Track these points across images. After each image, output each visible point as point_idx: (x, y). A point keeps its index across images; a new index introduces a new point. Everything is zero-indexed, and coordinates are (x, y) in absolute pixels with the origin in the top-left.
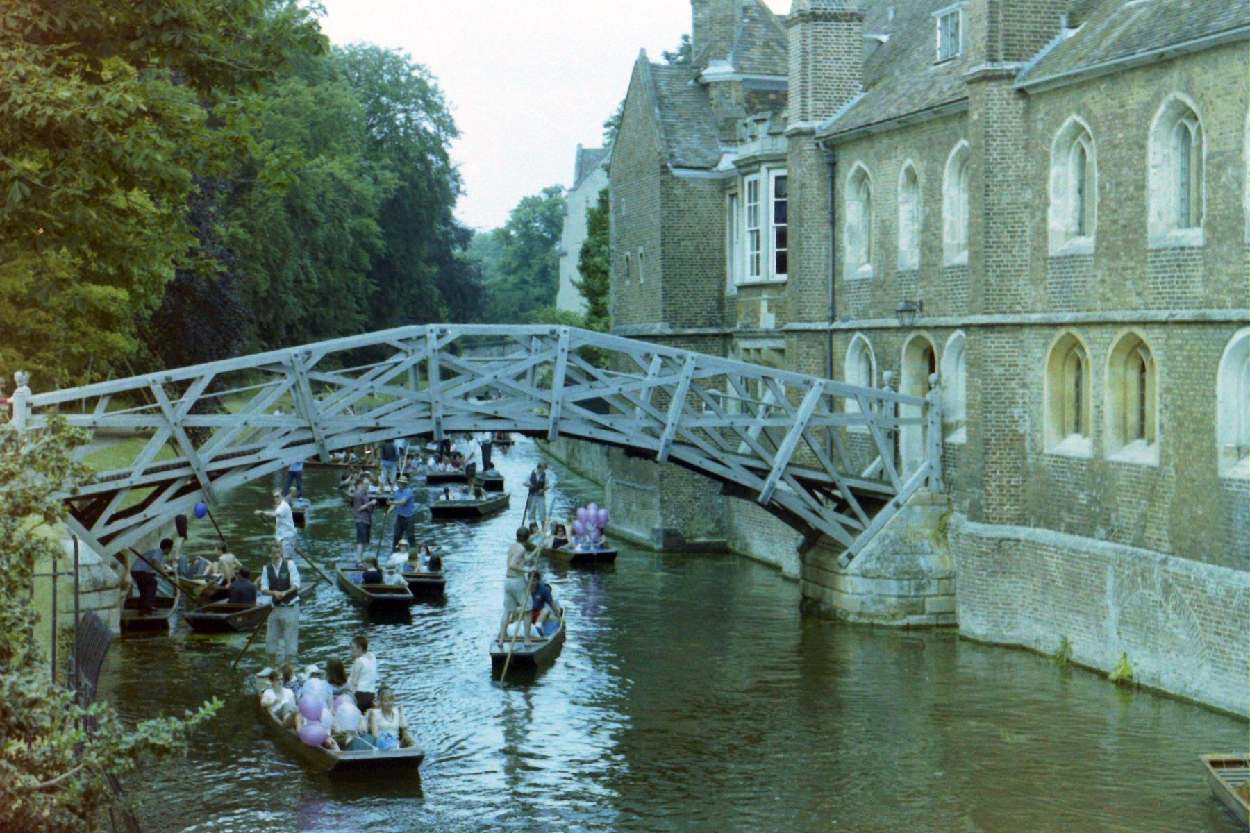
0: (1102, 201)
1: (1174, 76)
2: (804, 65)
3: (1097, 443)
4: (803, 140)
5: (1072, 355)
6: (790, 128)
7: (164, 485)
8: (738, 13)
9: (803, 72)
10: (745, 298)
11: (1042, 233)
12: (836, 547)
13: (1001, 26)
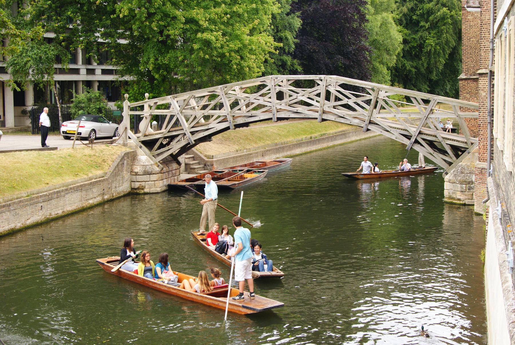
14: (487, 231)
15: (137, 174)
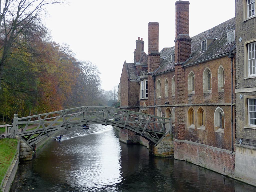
0: (196, 85)
1: (207, 64)
2: (150, 63)
3: (196, 126)
4: (150, 75)
5: (191, 111)
6: (148, 73)
7: (40, 133)
8: (141, 54)
9: (150, 65)
10: (141, 101)
11: (187, 91)
12: (154, 144)
13: (180, 56)
14: (235, 164)
15: (23, 152)
